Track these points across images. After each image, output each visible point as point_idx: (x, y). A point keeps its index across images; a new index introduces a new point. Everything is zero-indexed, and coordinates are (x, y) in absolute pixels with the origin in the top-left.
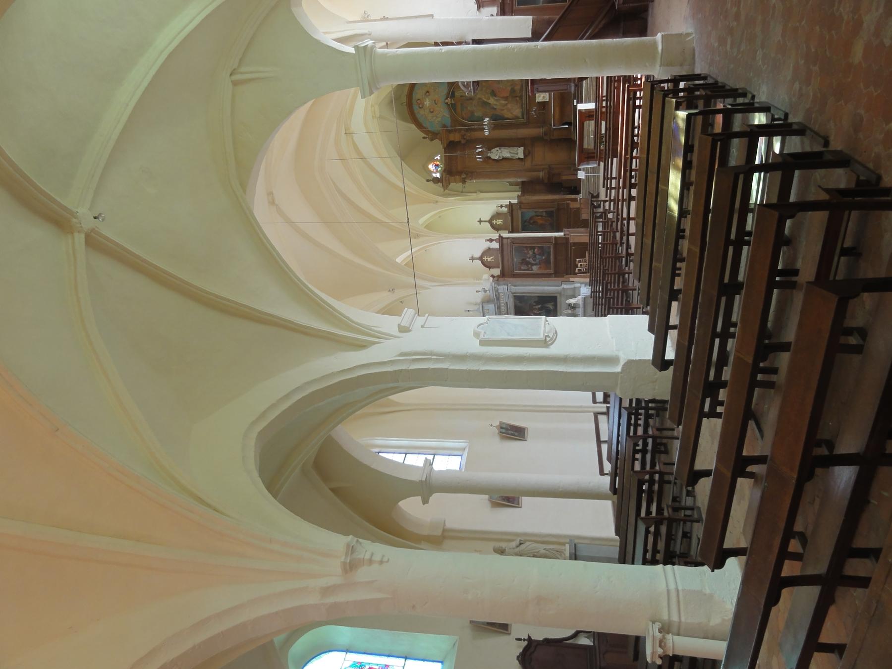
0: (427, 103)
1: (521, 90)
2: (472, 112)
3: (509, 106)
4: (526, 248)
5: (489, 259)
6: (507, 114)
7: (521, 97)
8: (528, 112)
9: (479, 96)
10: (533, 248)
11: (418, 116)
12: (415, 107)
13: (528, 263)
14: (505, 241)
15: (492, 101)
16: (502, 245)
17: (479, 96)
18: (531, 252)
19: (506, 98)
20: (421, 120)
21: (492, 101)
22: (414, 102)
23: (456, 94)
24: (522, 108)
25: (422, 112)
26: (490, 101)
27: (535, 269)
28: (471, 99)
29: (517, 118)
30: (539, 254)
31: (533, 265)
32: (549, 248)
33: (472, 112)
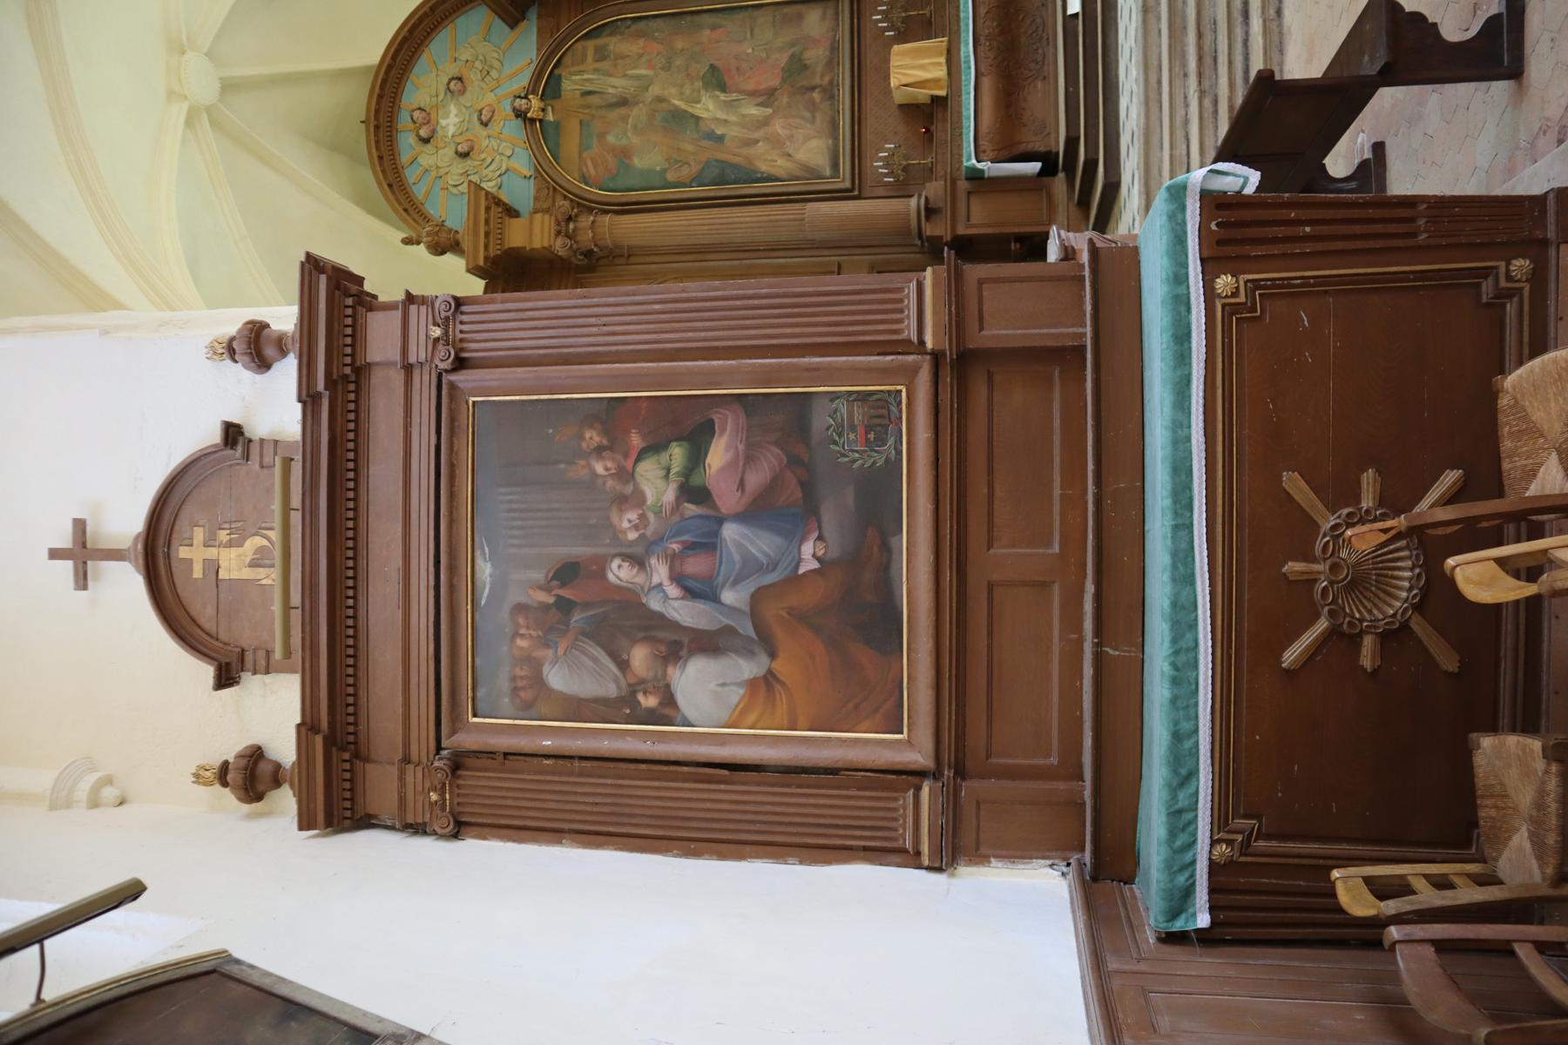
0: (451, 121)
1: (832, 63)
2: (624, 154)
3: (778, 127)
4: (611, 417)
5: (234, 563)
6: (769, 161)
7: (830, 93)
8: (857, 153)
9: (655, 90)
10: (689, 426)
11: (411, 175)
12: (407, 142)
13: (621, 622)
14: (381, 340)
15: (708, 107)
16: (338, 390)
17: (655, 90)
18: (656, 482)
19: (767, 97)
20: (419, 192)
21: (708, 107)
22: (404, 120)
23: (571, 84)
24: (834, 125)
25: (427, 158)
26: (698, 110)
27: (708, 700)
28: (623, 102)
29: (812, 173)
30: (757, 511)
31: (681, 646)
32: (880, 416)
33: (624, 154)
